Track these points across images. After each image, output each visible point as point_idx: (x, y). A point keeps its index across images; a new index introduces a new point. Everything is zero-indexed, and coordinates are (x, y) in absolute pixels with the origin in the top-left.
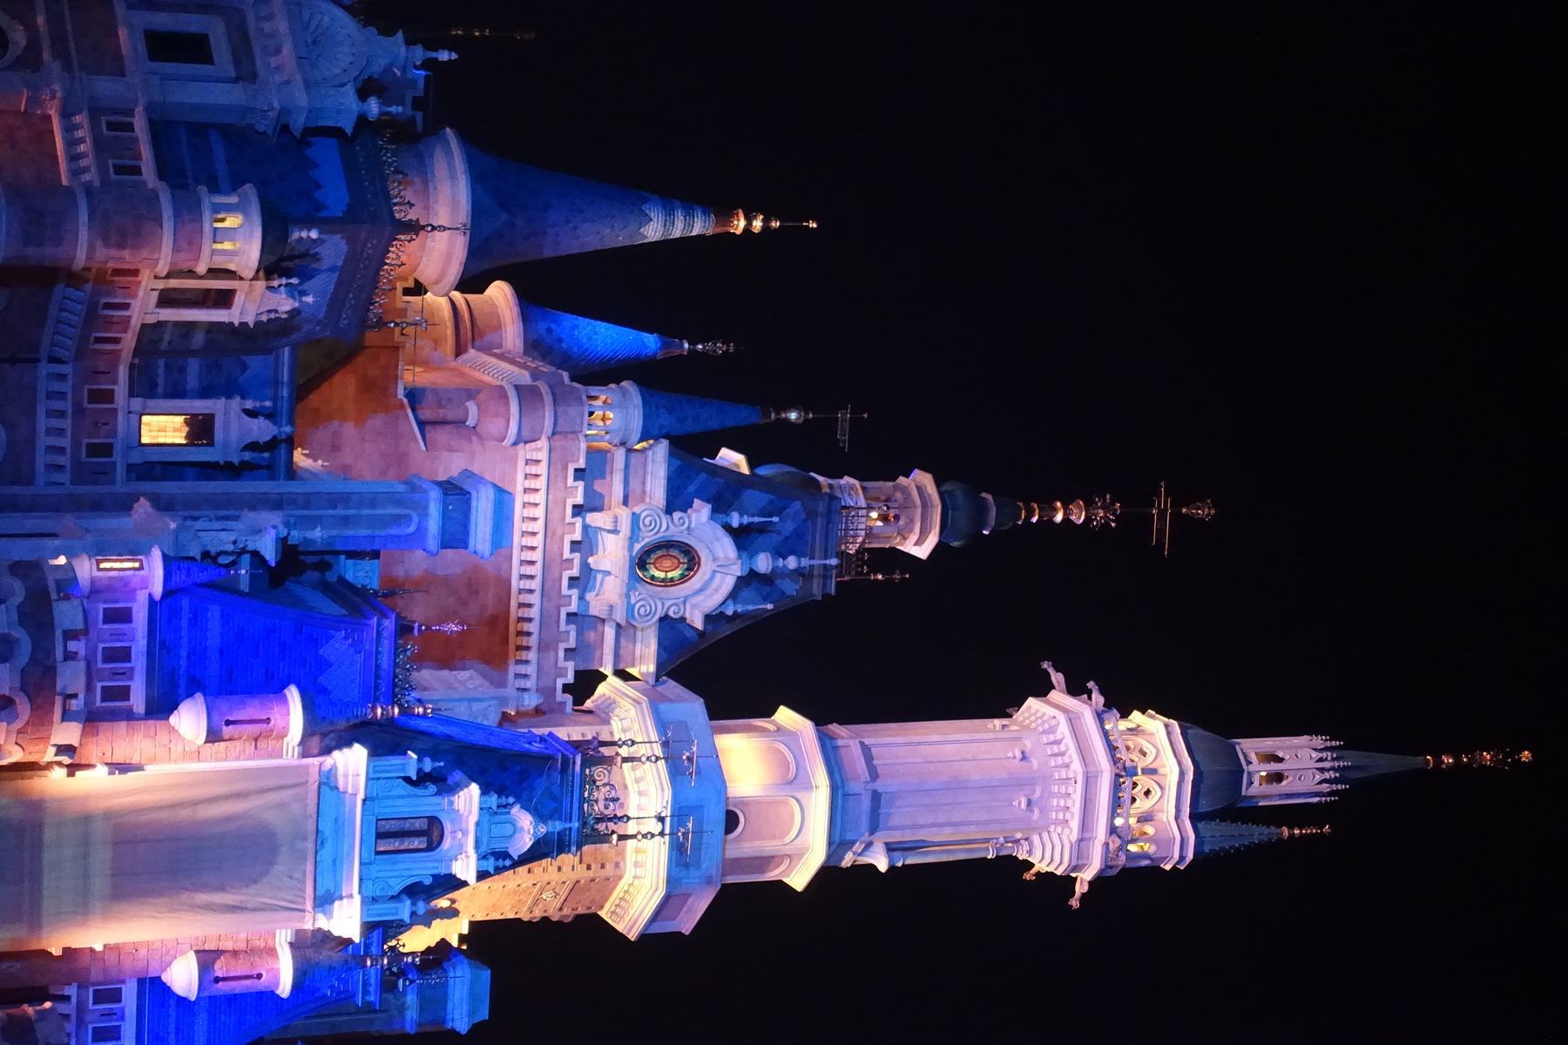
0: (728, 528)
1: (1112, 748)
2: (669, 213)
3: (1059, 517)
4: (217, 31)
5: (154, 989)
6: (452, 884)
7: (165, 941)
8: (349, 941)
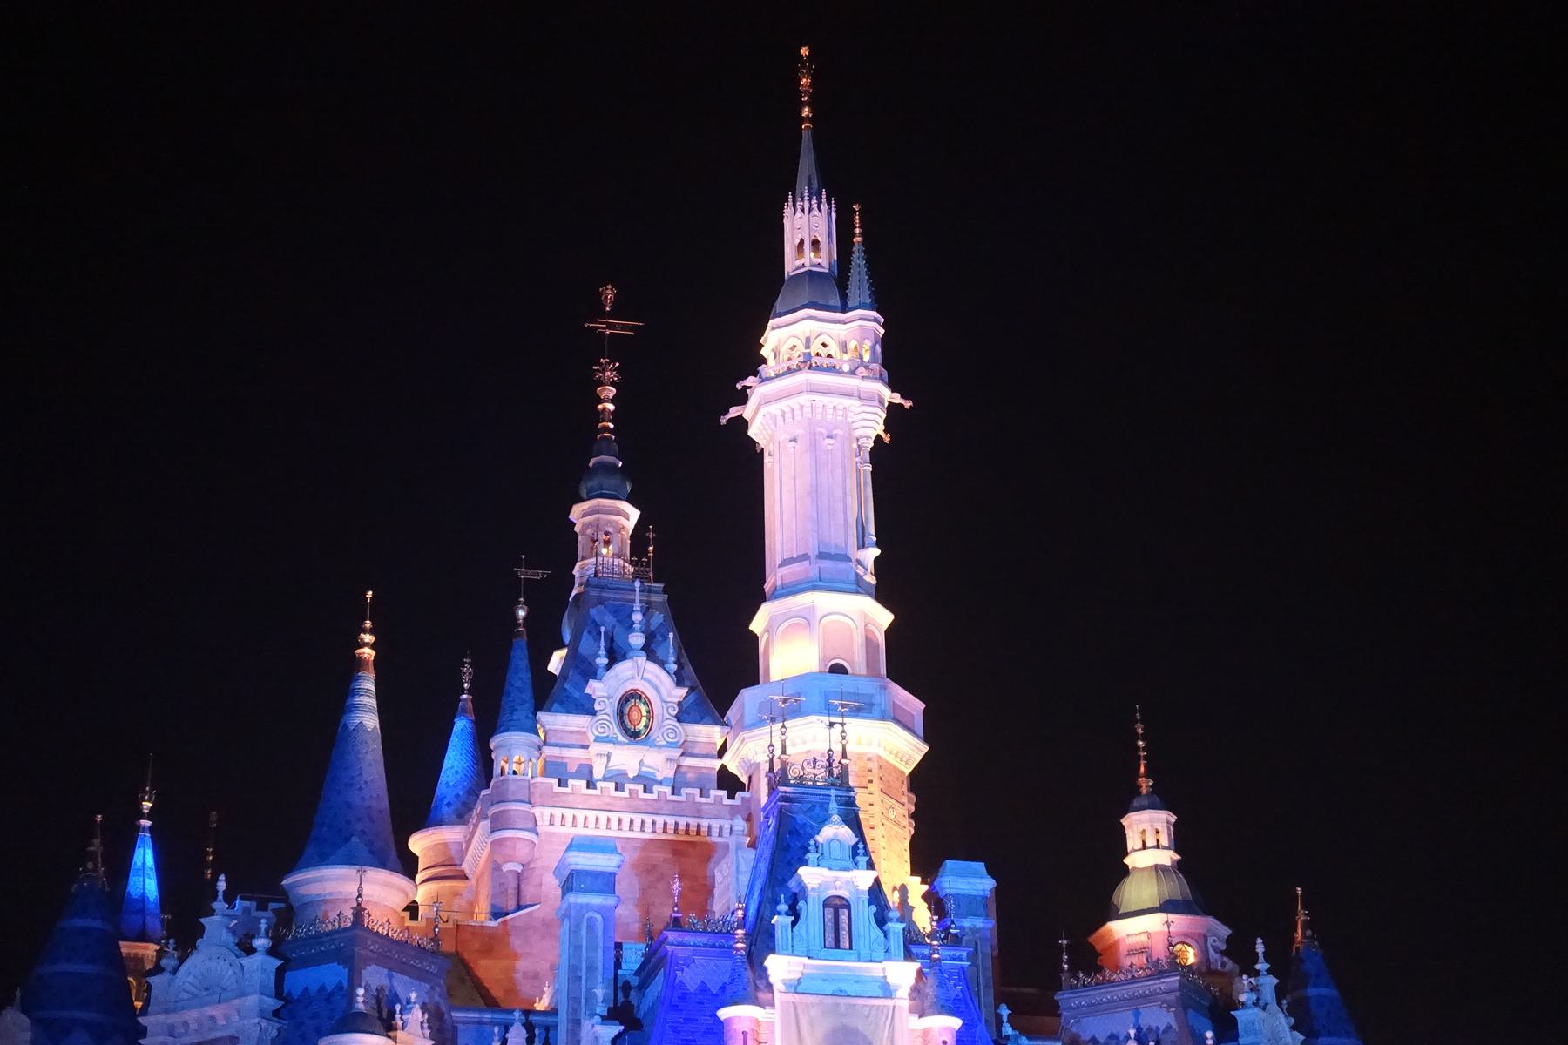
0: (609, 667)
1: (789, 371)
2: (354, 708)
3: (611, 407)
6: (876, 892)
8: (920, 972)
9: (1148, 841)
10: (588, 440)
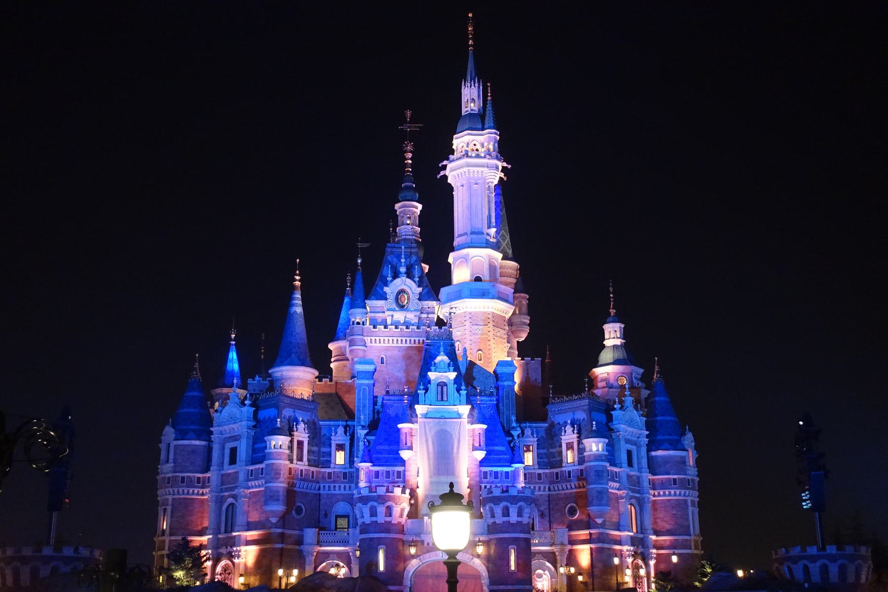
0: (391, 281)
3: (410, 162)
4: (229, 445)
5: (482, 463)
7: (467, 460)
9: (613, 335)
10: (402, 178)
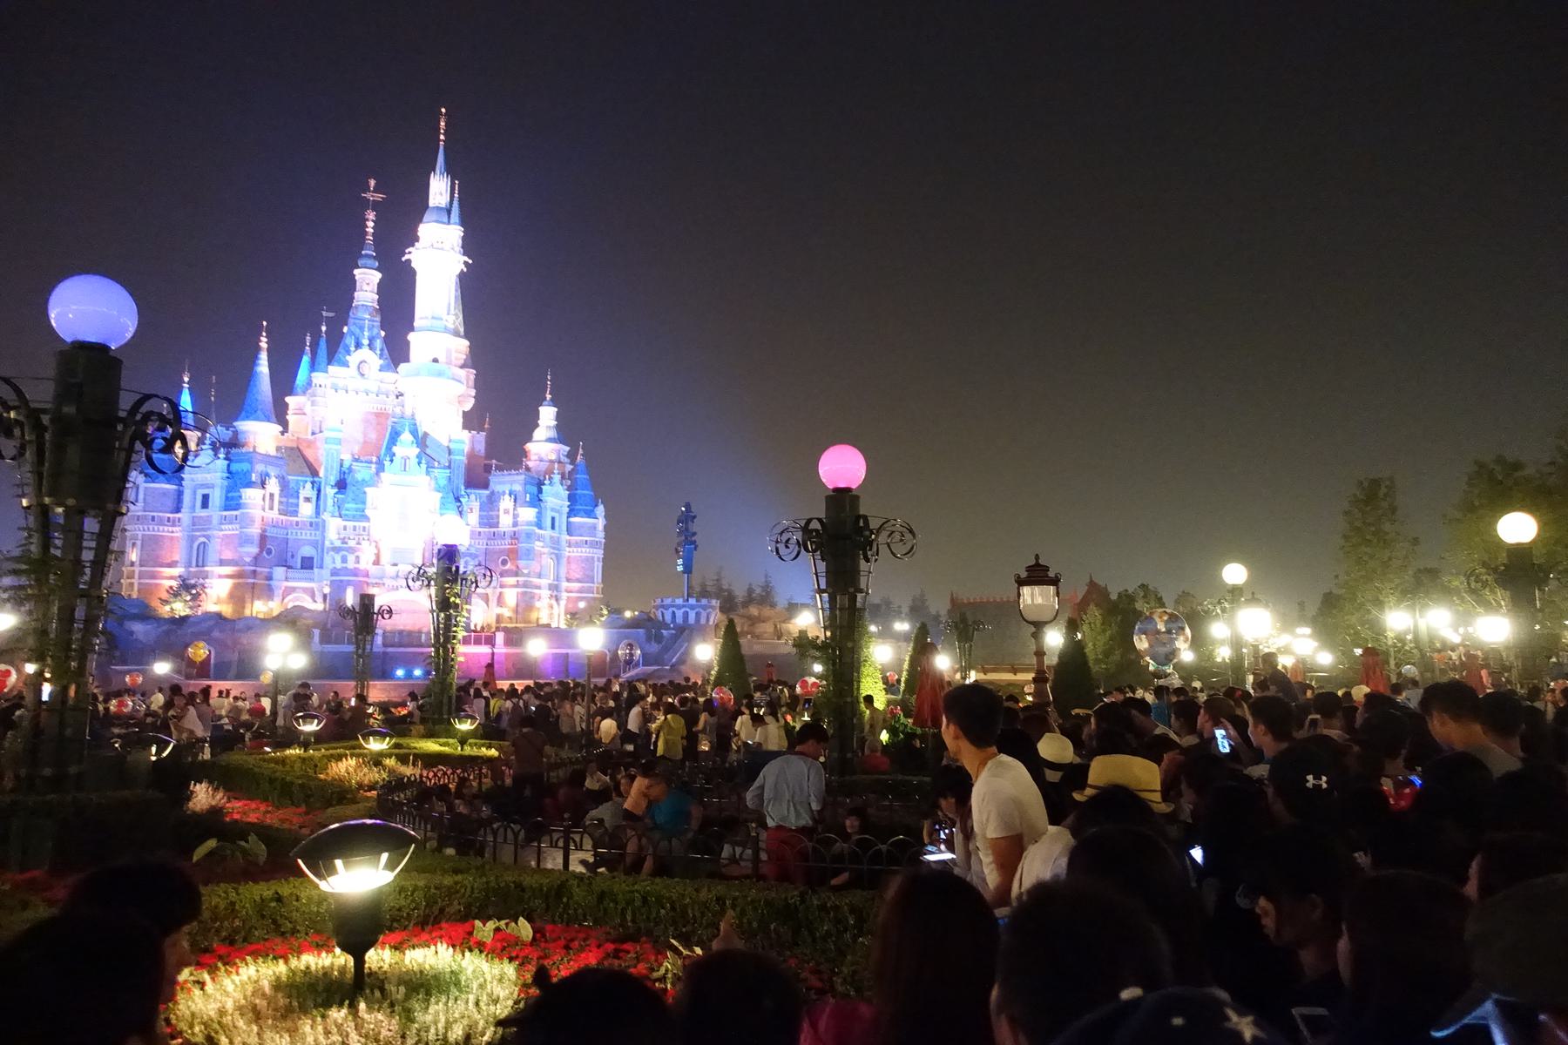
4: (201, 492)
9: (548, 415)
10: (361, 244)
